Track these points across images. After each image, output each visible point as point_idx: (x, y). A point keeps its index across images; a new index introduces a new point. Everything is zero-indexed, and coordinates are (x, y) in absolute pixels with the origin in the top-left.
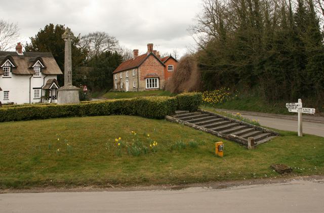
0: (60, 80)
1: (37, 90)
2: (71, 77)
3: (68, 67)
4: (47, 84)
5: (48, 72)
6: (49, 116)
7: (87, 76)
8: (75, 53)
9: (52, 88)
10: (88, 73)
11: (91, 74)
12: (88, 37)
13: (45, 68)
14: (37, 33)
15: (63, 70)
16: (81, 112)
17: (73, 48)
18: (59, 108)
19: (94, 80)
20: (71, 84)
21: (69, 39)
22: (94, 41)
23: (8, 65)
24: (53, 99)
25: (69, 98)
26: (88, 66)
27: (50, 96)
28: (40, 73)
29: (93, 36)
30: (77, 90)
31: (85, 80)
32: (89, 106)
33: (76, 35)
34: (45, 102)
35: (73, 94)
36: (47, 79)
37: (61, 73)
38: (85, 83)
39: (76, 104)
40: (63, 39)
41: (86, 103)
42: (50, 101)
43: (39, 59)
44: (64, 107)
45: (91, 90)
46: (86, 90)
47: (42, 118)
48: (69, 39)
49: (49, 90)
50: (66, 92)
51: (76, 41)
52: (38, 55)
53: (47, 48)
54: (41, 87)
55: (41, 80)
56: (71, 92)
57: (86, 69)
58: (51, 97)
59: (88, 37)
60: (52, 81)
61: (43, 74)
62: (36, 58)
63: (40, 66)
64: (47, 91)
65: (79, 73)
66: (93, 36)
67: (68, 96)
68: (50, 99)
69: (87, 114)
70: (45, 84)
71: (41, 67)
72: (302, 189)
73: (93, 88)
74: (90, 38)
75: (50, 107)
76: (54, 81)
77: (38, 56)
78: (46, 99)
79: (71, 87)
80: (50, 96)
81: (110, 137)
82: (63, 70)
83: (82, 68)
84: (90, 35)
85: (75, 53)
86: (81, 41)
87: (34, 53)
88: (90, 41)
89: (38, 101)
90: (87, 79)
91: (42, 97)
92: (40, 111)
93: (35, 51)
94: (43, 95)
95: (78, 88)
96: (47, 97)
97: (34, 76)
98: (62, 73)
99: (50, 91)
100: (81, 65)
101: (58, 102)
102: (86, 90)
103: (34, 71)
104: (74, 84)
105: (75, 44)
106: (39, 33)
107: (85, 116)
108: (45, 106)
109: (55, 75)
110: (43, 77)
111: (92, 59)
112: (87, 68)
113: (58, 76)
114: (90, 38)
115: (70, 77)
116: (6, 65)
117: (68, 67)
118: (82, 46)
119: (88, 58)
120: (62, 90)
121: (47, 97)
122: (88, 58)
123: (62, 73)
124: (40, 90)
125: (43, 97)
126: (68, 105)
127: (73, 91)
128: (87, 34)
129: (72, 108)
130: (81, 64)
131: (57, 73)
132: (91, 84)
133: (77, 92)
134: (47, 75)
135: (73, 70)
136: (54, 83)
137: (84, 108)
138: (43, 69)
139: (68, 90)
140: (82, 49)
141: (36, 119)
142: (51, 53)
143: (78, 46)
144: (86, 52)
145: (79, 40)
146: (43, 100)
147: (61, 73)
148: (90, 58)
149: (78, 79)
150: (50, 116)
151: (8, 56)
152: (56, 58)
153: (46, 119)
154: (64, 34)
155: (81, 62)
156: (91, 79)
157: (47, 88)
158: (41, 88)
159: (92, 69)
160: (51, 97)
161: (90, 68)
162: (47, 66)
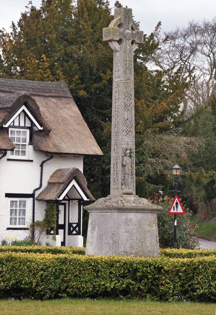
0: (97, 176)
1: (18, 199)
2: (131, 168)
3: (123, 137)
4: (49, 183)
5: (55, 146)
6: (59, 291)
7: (184, 167)
8: (146, 87)
9: (68, 198)
10: (184, 155)
11: (196, 161)
12: (185, 36)
13: (46, 132)
14: (17, 18)
15: (104, 141)
16: (167, 285)
17: (139, 70)
18: (94, 267)
19: (205, 181)
20: (133, 190)
21: (127, 44)
22: (206, 49)
23: (22, 124)
24: (70, 233)
25: (123, 236)
26: (184, 133)
27: (61, 222)
28: (29, 149)
29: (202, 32)
30: (152, 211)
31: (176, 177)
32: (193, 270)
33: (147, 29)
34: (44, 240)
35: (140, 223)
36: (51, 168)
37: (96, 150)
38: (175, 189)
39: (150, 260)
40: (106, 44)
41: (178, 257)
42: (59, 238)
43: (26, 101)
44: (111, 264)
45: (195, 212)
46: (180, 210)
47: (40, 297)
48: (127, 44)
49: (57, 203)
50: (116, 215)
51: (148, 47)
52: (23, 87)
53: (52, 67)
54: (31, 192)
55: (34, 168)
56: (132, 216)
57: (180, 143)
58: (62, 227)
59: (185, 36)
60: (67, 173)
61: (37, 150)
62: (14, 97)
63: (28, 124)
64: (53, 206)
65: (155, 155)
66: (202, 32)
67: (123, 231)
68: (61, 231)
69: (185, 292)
70: (45, 184)
71: (31, 129)
72: (210, 308)
73: (201, 205)
74: (191, 39)
75: (64, 262)
76: (74, 175)
77: (23, 93)
78: (48, 233)
79: (133, 200)
80: (61, 222)
81: (29, 261)
82: (104, 141)
83: (166, 137)
84: (194, 29)
85: (146, 87)
86: (165, 47)
87: (9, 82)
88: (193, 51)
89: (22, 236)
90: (183, 177)
91: (34, 225)
92: (33, 272)
93: (11, 75)
94: (40, 217)
95: (155, 207)
96: (51, 226)
97: (9, 155)
98: (99, 152)
99: (61, 208)
100: (163, 130)
101: (94, 247)
102: (180, 210)
103: (10, 140)
104: (140, 191)
105: (145, 60)
106: (24, 16)
107: (180, 300)
108: (50, 256)
109: (75, 156)
110: (37, 161)
111: (199, 112)
112: (183, 139)
113: (88, 160)
114: (191, 39)
115: (128, 169)
116: (16, 124)
117: (123, 137)
118: (167, 68)
119: (188, 106)
120: (102, 209)
121: (51, 226)
122: (188, 106)
123: (99, 152)
124: (29, 201)
125: (38, 224)
126: (124, 258)
127: (140, 216)
128: (184, 26)
129: (136, 270)
130: (160, 124)
131: (83, 151)
132: (197, 194)
133: (153, 218)
134: (50, 156)
135: (138, 144)
136: (74, 182)
137: (175, 272)
138: (39, 135)
139: (122, 210)
140: (165, 78)
141: (18, 298)
142: (63, 84)
143: (151, 66)
144: (179, 87)
145: (155, 46)
146: (37, 233)
147: (96, 150)
148: (190, 104)
149: (152, 174)
150: (65, 291)
151: (25, 96)
152: (79, 101)
153: (50, 298)
154: (112, 25)
155: (161, 119)
156: (195, 176)
157: (51, 196)
158: (31, 196)
159: (199, 142)
160: (62, 227)
161: (193, 139)
162: (51, 126)
